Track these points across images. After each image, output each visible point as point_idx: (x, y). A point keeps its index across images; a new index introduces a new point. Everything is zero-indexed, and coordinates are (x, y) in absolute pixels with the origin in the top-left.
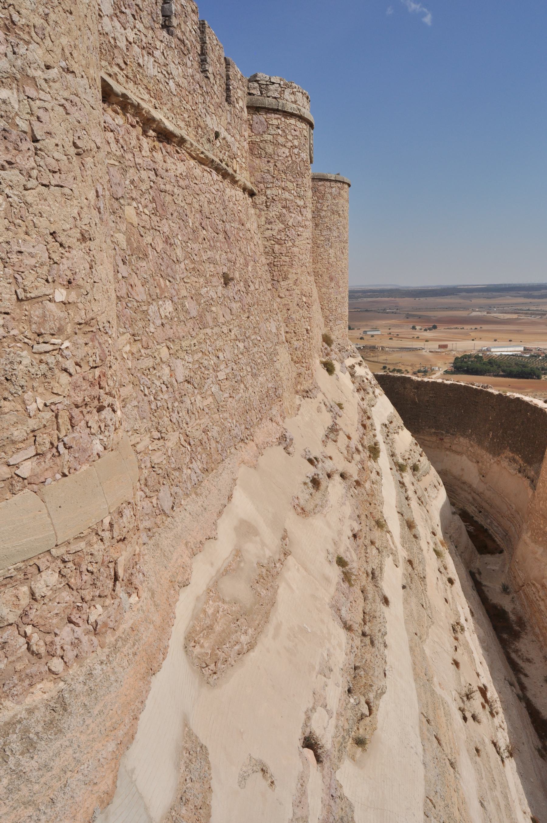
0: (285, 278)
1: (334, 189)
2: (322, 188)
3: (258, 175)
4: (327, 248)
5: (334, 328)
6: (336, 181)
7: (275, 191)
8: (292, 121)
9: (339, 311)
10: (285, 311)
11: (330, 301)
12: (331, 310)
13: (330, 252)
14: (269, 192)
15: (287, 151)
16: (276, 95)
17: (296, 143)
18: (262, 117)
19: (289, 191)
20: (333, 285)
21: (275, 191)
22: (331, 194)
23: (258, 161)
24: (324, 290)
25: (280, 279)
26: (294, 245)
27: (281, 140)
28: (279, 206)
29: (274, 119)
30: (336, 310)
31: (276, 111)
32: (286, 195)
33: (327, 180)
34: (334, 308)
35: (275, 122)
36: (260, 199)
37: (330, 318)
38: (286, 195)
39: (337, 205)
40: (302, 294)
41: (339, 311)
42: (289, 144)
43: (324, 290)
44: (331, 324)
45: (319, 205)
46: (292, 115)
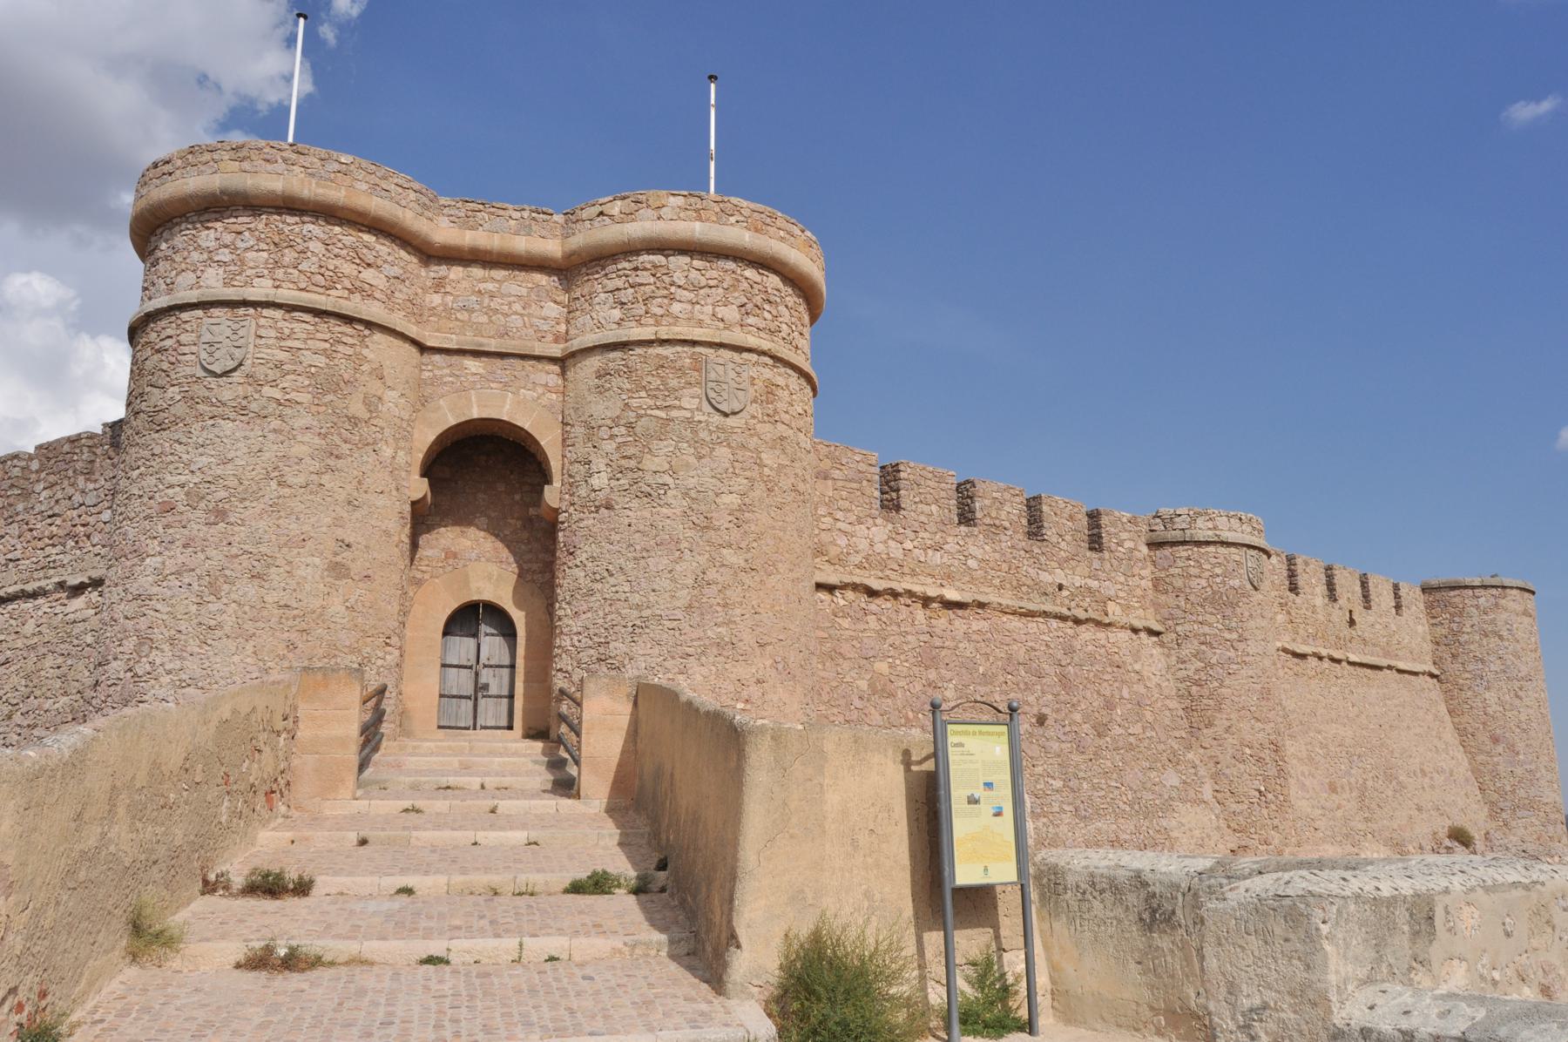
0: (1210, 725)
1: (1482, 600)
2: (1456, 600)
3: (1165, 612)
4: (1481, 690)
5: (1513, 824)
6: (1485, 587)
7: (1187, 627)
8: (1211, 549)
9: (1522, 793)
10: (1211, 765)
11: (1496, 775)
12: (1502, 793)
13: (1487, 695)
14: (1179, 628)
15: (1204, 583)
16: (1184, 526)
17: (1218, 571)
18: (1167, 551)
19: (1210, 625)
20: (1500, 749)
21: (1187, 627)
22: (1477, 607)
23: (1163, 597)
24: (1480, 758)
25: (1202, 726)
26: (1221, 686)
27: (1193, 571)
28: (1196, 642)
29: (1182, 552)
30: (1513, 792)
31: (1184, 543)
32: (1206, 629)
33: (1466, 587)
34: (1508, 788)
35: (1185, 554)
36: (1165, 638)
37: (1501, 805)
38: (1206, 629)
39: (1493, 622)
40: (1242, 744)
41: (1522, 793)
42: (1207, 574)
43: (1480, 758)
44: (1504, 815)
45: (1454, 626)
46: (1208, 543)
